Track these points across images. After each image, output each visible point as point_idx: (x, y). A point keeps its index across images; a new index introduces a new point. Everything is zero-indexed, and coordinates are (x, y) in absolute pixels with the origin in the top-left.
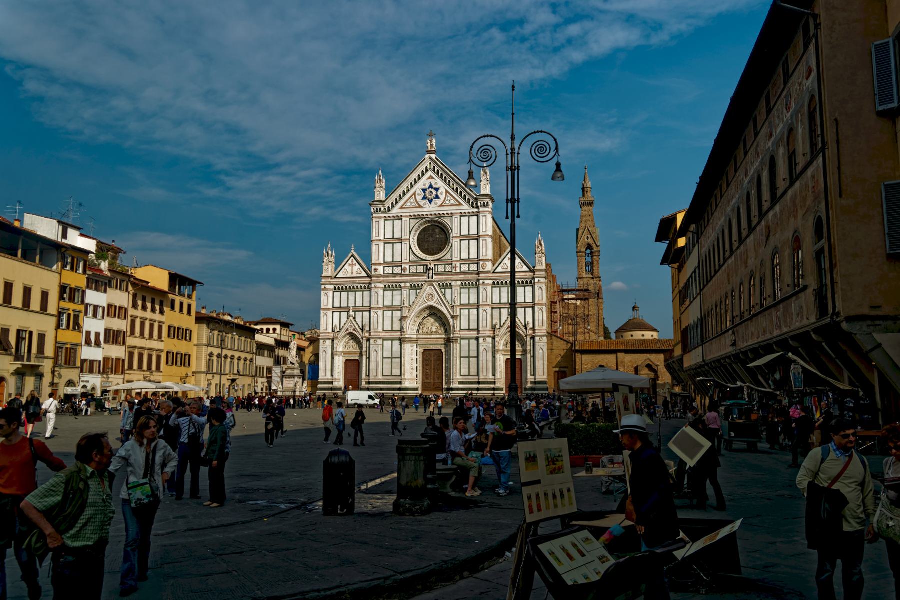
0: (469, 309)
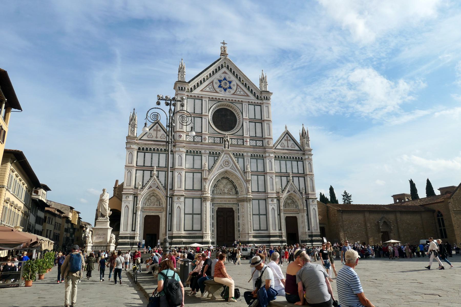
0: (258, 175)
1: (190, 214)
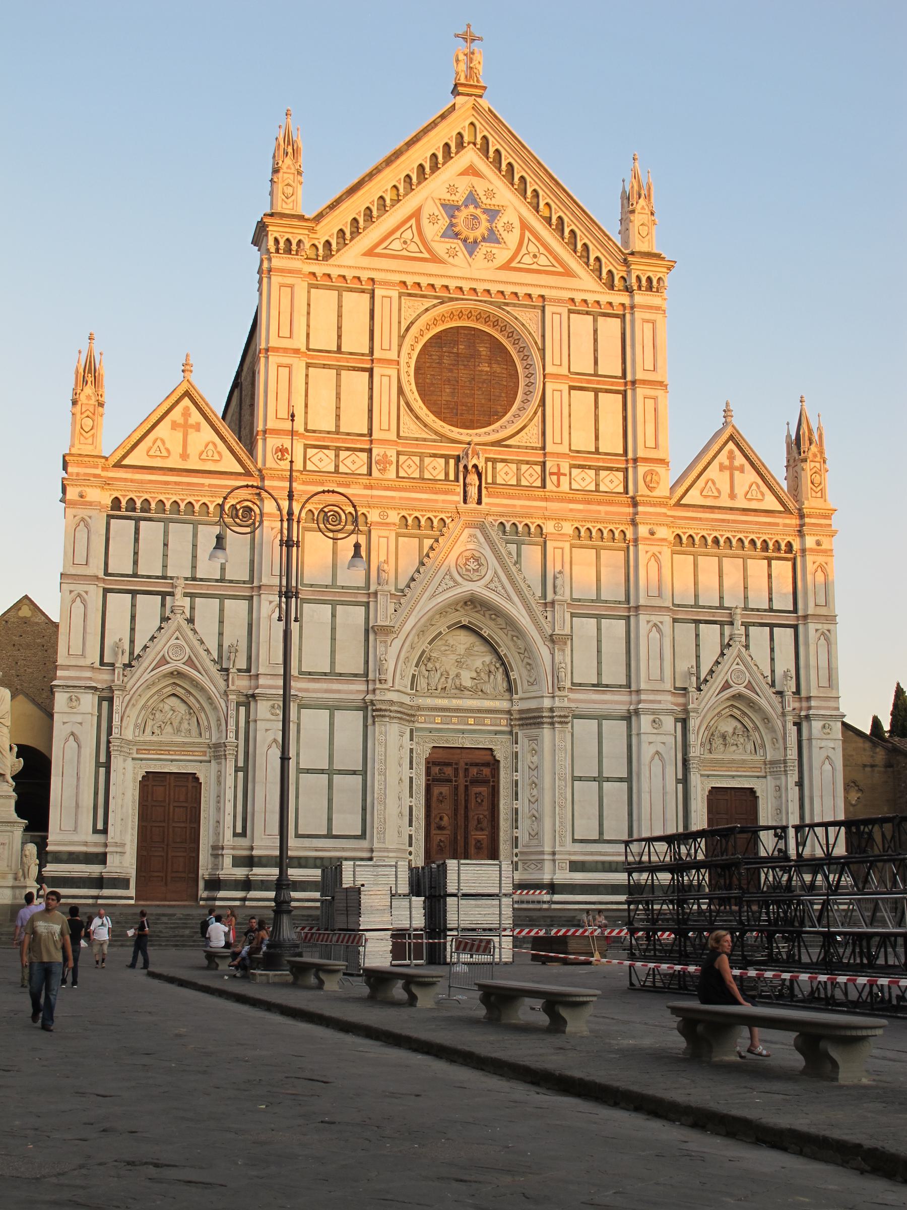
0: (599, 617)
1: (322, 771)
